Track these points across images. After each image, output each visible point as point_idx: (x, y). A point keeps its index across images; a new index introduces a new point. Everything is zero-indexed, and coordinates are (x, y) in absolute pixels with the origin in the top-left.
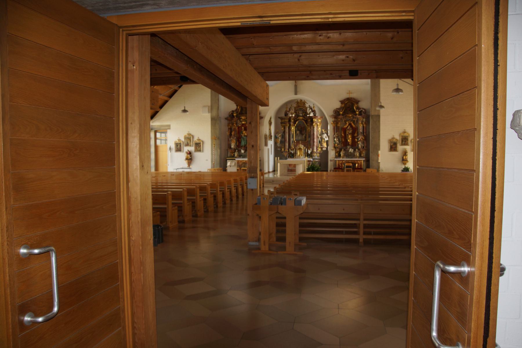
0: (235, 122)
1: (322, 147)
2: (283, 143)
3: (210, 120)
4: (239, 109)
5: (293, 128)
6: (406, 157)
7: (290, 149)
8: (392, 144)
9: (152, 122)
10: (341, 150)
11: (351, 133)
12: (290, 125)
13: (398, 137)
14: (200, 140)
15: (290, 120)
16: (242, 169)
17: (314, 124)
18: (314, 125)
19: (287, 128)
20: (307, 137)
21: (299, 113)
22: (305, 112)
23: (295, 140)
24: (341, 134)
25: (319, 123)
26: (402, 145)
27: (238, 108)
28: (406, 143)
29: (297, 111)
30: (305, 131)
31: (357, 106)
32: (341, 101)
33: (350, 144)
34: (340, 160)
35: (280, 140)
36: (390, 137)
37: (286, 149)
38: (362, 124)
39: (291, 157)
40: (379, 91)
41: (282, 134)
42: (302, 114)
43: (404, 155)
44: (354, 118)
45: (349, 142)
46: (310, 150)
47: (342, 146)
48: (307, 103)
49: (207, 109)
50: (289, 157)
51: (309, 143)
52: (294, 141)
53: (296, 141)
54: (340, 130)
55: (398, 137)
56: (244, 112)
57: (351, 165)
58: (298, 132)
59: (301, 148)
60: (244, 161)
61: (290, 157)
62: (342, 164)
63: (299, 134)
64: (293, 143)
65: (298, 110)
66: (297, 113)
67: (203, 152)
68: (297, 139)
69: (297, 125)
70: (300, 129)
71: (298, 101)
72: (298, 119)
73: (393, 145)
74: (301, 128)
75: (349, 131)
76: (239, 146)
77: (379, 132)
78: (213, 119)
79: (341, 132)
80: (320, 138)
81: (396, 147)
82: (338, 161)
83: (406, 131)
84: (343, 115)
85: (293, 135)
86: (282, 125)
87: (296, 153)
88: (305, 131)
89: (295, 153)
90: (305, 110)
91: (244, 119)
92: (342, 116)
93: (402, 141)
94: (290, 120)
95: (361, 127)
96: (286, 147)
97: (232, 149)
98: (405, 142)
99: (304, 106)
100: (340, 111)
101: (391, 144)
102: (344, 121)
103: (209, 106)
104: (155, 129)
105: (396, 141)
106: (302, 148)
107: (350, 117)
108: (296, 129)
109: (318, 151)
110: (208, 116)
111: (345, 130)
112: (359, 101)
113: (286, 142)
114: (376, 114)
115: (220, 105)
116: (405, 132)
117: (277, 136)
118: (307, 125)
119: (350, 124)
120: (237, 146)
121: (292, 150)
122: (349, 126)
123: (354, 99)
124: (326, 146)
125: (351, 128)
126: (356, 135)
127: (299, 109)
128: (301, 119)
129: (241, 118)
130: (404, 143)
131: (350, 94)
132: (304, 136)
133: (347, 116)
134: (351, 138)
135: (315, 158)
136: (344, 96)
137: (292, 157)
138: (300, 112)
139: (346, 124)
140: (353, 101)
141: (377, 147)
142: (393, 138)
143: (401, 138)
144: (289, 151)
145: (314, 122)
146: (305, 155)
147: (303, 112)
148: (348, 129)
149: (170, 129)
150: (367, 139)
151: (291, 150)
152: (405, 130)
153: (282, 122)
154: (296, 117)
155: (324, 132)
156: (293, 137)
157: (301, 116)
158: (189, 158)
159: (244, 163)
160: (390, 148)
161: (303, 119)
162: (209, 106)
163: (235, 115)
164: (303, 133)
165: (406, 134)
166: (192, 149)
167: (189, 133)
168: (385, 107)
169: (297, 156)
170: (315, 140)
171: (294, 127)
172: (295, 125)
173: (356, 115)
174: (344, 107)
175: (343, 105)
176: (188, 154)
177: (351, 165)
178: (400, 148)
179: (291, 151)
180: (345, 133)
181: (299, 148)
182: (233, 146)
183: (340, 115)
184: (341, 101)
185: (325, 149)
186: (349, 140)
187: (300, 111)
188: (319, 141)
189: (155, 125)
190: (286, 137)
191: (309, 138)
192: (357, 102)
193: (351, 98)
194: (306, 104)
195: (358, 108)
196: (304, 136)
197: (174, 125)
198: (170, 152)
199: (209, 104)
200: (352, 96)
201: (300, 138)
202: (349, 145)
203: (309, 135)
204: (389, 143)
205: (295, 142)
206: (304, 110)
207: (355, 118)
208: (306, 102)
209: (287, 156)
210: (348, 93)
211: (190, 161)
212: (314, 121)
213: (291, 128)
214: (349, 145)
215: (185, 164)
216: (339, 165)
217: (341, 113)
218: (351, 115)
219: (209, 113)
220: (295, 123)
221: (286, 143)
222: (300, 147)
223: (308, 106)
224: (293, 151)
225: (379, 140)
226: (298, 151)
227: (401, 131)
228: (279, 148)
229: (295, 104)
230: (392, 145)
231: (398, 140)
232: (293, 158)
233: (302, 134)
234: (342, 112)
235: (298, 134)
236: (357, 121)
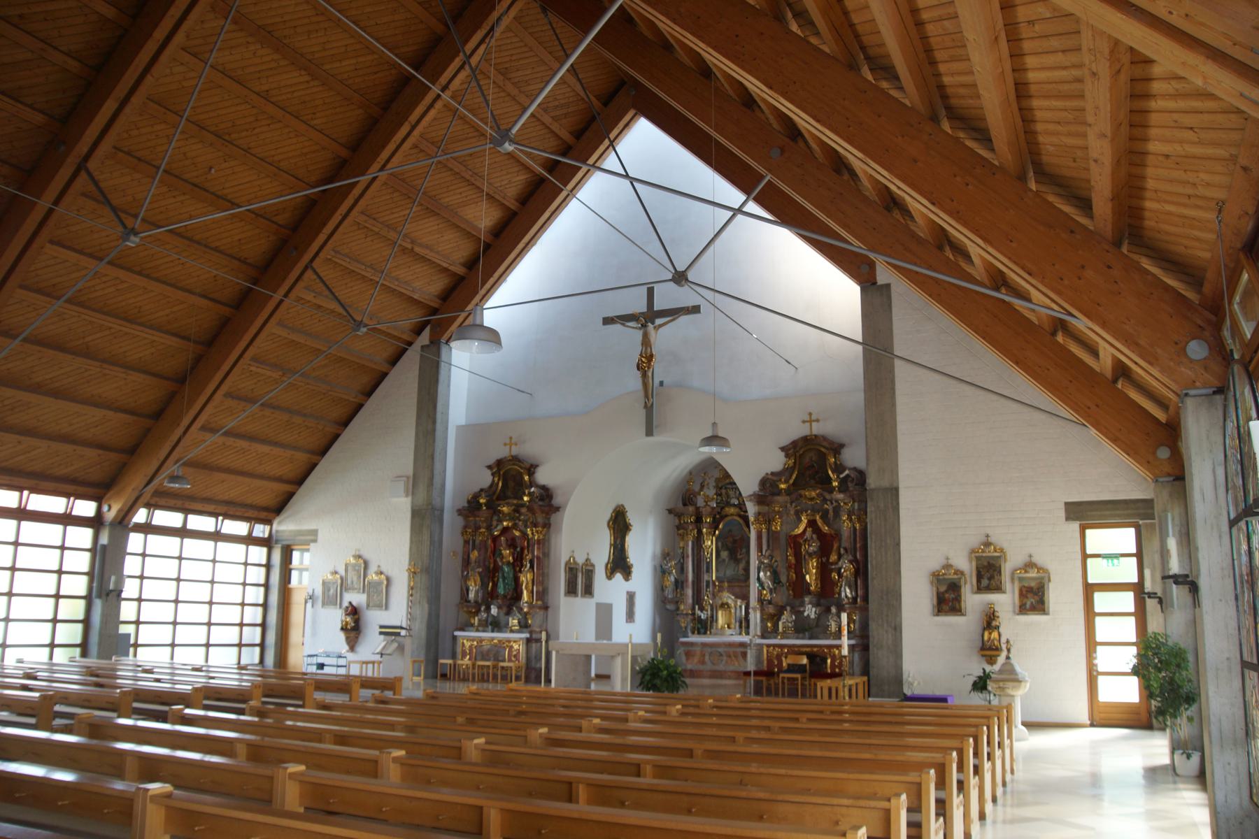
0: (483, 522)
3: (409, 515)
4: (498, 483)
5: (710, 543)
6: (990, 634)
8: (943, 589)
9: (280, 523)
10: (780, 611)
11: (815, 552)
12: (700, 532)
13: (963, 563)
14: (381, 573)
15: (699, 520)
16: (479, 666)
19: (690, 543)
21: (728, 496)
23: (717, 577)
24: (787, 556)
26: (980, 589)
27: (496, 479)
28: (992, 582)
29: (723, 491)
30: (744, 550)
31: (835, 462)
32: (782, 449)
33: (812, 588)
34: (775, 646)
35: (672, 579)
36: (935, 564)
38: (851, 520)
39: (699, 633)
40: (894, 405)
43: (984, 629)
44: (825, 500)
45: (809, 585)
47: (789, 595)
49: (401, 486)
50: (693, 633)
52: (714, 583)
54: (783, 541)
55: (963, 563)
56: (509, 494)
57: (805, 661)
58: (725, 554)
59: (727, 604)
60: (495, 641)
62: (779, 657)
63: (727, 560)
64: (708, 586)
65: (726, 488)
67: (387, 608)
68: (721, 575)
72: (723, 513)
73: (946, 591)
74: (735, 541)
75: (809, 546)
76: (490, 597)
77: (898, 544)
78: (416, 514)
79: (787, 551)
81: (958, 599)
82: (768, 646)
83: (991, 540)
84: (788, 492)
85: (709, 565)
87: (713, 619)
89: (712, 617)
91: (509, 514)
92: (787, 498)
93: (979, 577)
95: (846, 525)
97: (469, 602)
98: (990, 578)
100: (780, 480)
101: (938, 589)
102: (792, 512)
103: (408, 478)
104: (282, 540)
105: (955, 577)
106: (730, 601)
107: (812, 499)
108: (720, 544)
110: (403, 505)
111: (795, 543)
112: (842, 446)
113: (685, 585)
114: (885, 483)
115: (436, 472)
116: (988, 544)
119: (812, 523)
120: (488, 594)
122: (809, 530)
123: (824, 438)
125: (814, 536)
126: (833, 558)
127: (728, 484)
128: (732, 515)
129: (500, 512)
130: (985, 582)
131: (814, 424)
132: (742, 565)
133: (801, 496)
134: (817, 568)
136: (797, 431)
137: (702, 631)
139: (800, 520)
140: (824, 447)
141: (893, 597)
142: (948, 566)
143: (974, 564)
144: (693, 614)
146: (741, 627)
148: (805, 541)
149: (315, 541)
150: (861, 571)
152: (988, 536)
156: (709, 570)
157: (734, 505)
158: (349, 627)
159: (495, 645)
160: (935, 602)
162: (408, 478)
163: (482, 501)
164: (739, 557)
165: (990, 552)
166: (358, 598)
167: (357, 553)
168: (731, 443)
169: (717, 628)
171: (714, 539)
172: (717, 532)
173: (831, 490)
174: (793, 468)
175: (791, 462)
176: (346, 615)
177: (805, 661)
178: (973, 601)
180: (798, 555)
181: (720, 602)
182: (472, 596)
183: (779, 492)
184: (782, 449)
186: (807, 577)
189: (283, 531)
192: (837, 448)
193: (816, 436)
195: (839, 468)
196: (742, 565)
197: (325, 529)
198: (313, 606)
199: (410, 472)
200: (817, 429)
201: (729, 572)
202: (809, 592)
204: (932, 583)
207: (828, 503)
209: (686, 628)
210: (804, 422)
211: (352, 634)
214: (809, 592)
215: (339, 642)
216: (770, 661)
217: (783, 486)
218: (814, 494)
219: (407, 496)
220: (716, 528)
221: (687, 586)
222: (725, 600)
225: (898, 573)
226: (720, 613)
227: (975, 540)
228: (671, 602)
230: (943, 593)
231: (962, 573)
232: (705, 633)
233: (737, 561)
234: (786, 482)
235: (724, 560)
236: (837, 511)
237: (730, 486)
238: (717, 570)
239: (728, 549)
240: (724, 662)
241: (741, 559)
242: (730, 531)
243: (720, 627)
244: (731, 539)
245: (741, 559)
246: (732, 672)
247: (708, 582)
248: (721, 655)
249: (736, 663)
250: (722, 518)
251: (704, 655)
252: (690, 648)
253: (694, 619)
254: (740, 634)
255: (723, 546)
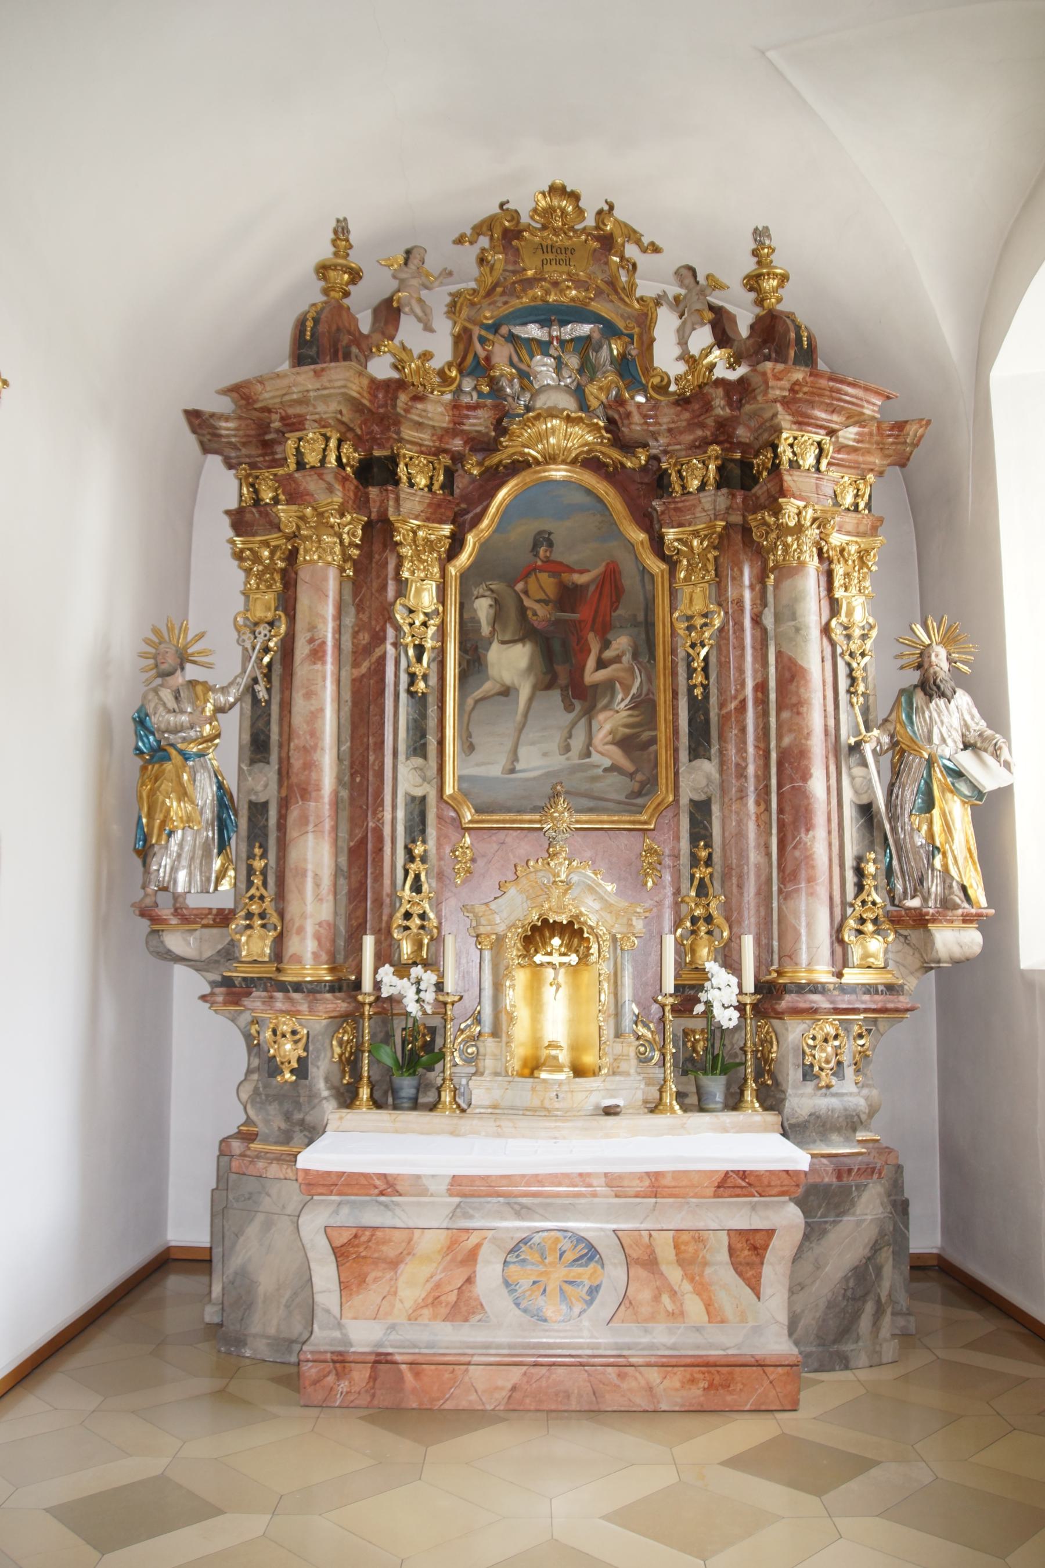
1: (915, 903)
2: (257, 834)
7: (369, 942)
17: (791, 507)
18: (799, 529)
20: (663, 732)
21: (525, 376)
22: (623, 365)
25: (851, 519)
29: (501, 353)
30: (621, 643)
35: (206, 793)
37: (293, 946)
41: (251, 690)
42: (579, 393)
46: (731, 963)
48: (656, 249)
50: (347, 1098)
51: (700, 833)
53: (478, 811)
61: (364, 1093)
63: (524, 692)
64: (417, 827)
66: (502, 368)
69: (484, 547)
70: (541, 613)
71: (515, 215)
80: (868, 749)
86: (239, 556)
88: (621, 643)
90: (621, 324)
94: (393, 460)
96: (293, 909)
99: (612, 283)
108: (483, 608)
109: (852, 976)
113: (294, 814)
117: (159, 719)
118: (658, 544)
121: (402, 970)
124: (978, 893)
128: (551, 459)
135: (823, 1103)
137: (407, 1085)
138: (543, 368)
145: (790, 479)
147: (587, 368)
151: (385, 955)
153: (257, 501)
154: (479, 422)
155: (940, 659)
161: (590, 463)
164: (592, 676)
170: (818, 785)
179: (386, 972)
185: (971, 940)
187: (543, 347)
188: (866, 811)
190: (316, 715)
191: (699, 748)
194: (631, 251)
203: (698, 708)
205: (468, 815)
206: (610, 330)
208: (633, 235)
212: (794, 465)
213: (402, 587)
223: (674, 290)
224: (429, 978)
228: (187, 918)
229: (471, 252)
235: (507, 692)
237: (534, 331)
238: (468, 746)
239: (527, 632)
240: (608, 1300)
241: (609, 686)
242: (542, 539)
243: (516, 1064)
244: (547, 580)
245: (609, 686)
246: (667, 1364)
247: (418, 807)
248: (590, 1253)
249: (694, 1307)
250: (495, 478)
251: (471, 1257)
252: (371, 1217)
253: (352, 1017)
254: (655, 1108)
255: (498, 617)
